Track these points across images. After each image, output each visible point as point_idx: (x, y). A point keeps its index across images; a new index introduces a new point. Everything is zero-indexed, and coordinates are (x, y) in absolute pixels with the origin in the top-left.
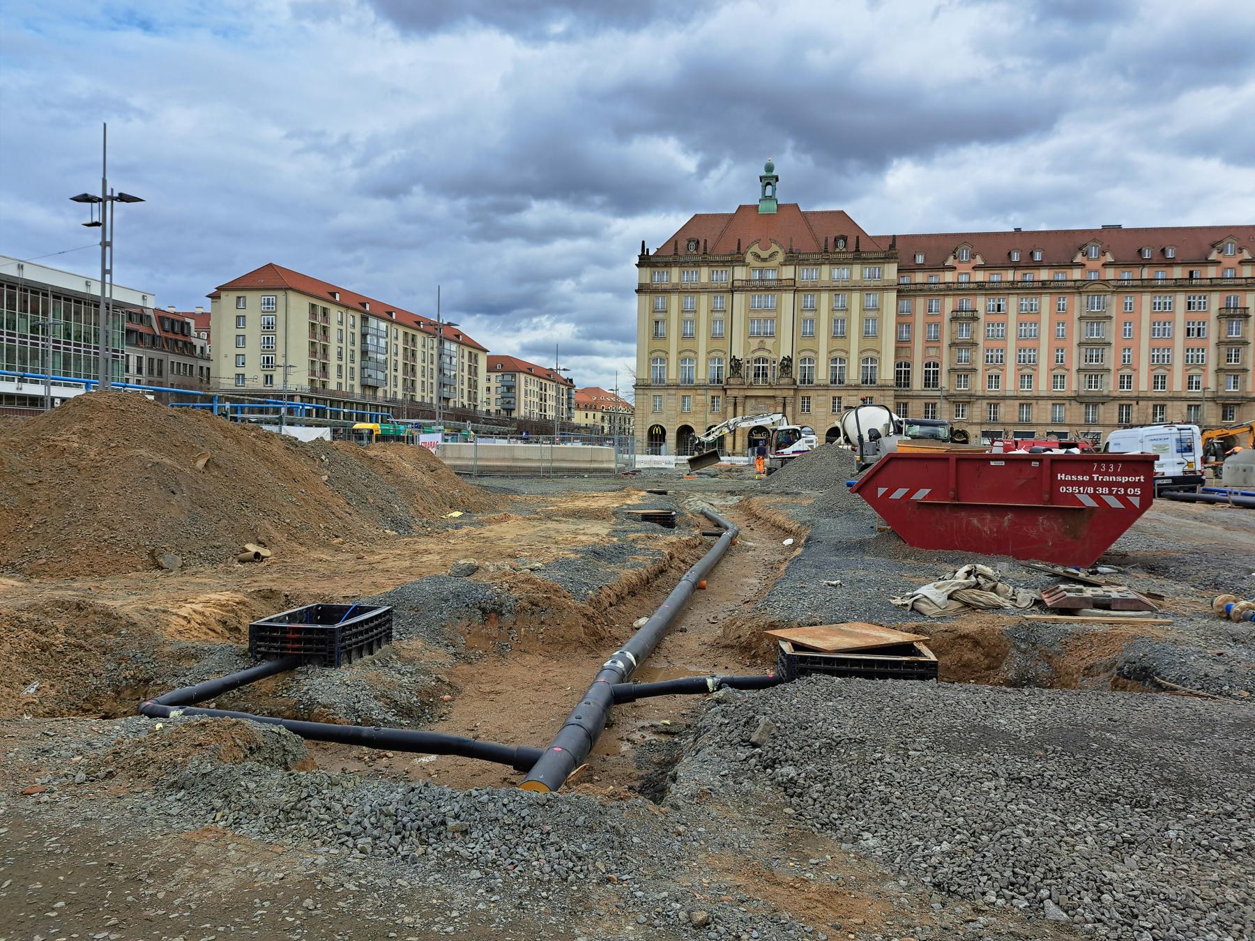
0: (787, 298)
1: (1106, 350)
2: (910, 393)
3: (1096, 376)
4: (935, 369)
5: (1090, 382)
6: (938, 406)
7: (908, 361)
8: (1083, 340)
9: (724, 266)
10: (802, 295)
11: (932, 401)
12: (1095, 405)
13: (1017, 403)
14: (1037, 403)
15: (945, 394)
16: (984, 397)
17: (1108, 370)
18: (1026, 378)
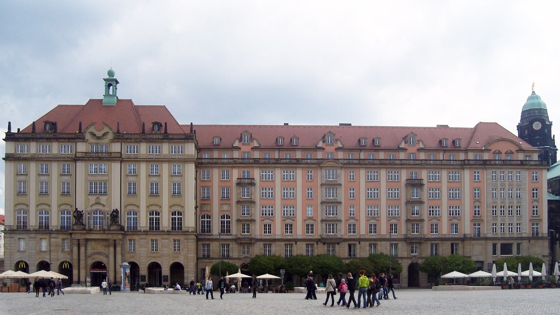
0: (116, 166)
1: (338, 207)
2: (211, 237)
3: (333, 225)
4: (228, 220)
5: (329, 229)
6: (231, 246)
7: (209, 214)
8: (324, 200)
9: (69, 142)
10: (127, 165)
11: (226, 243)
12: (333, 244)
13: (283, 243)
14: (296, 243)
15: (234, 237)
16: (261, 240)
17: (340, 221)
18: (289, 227)
